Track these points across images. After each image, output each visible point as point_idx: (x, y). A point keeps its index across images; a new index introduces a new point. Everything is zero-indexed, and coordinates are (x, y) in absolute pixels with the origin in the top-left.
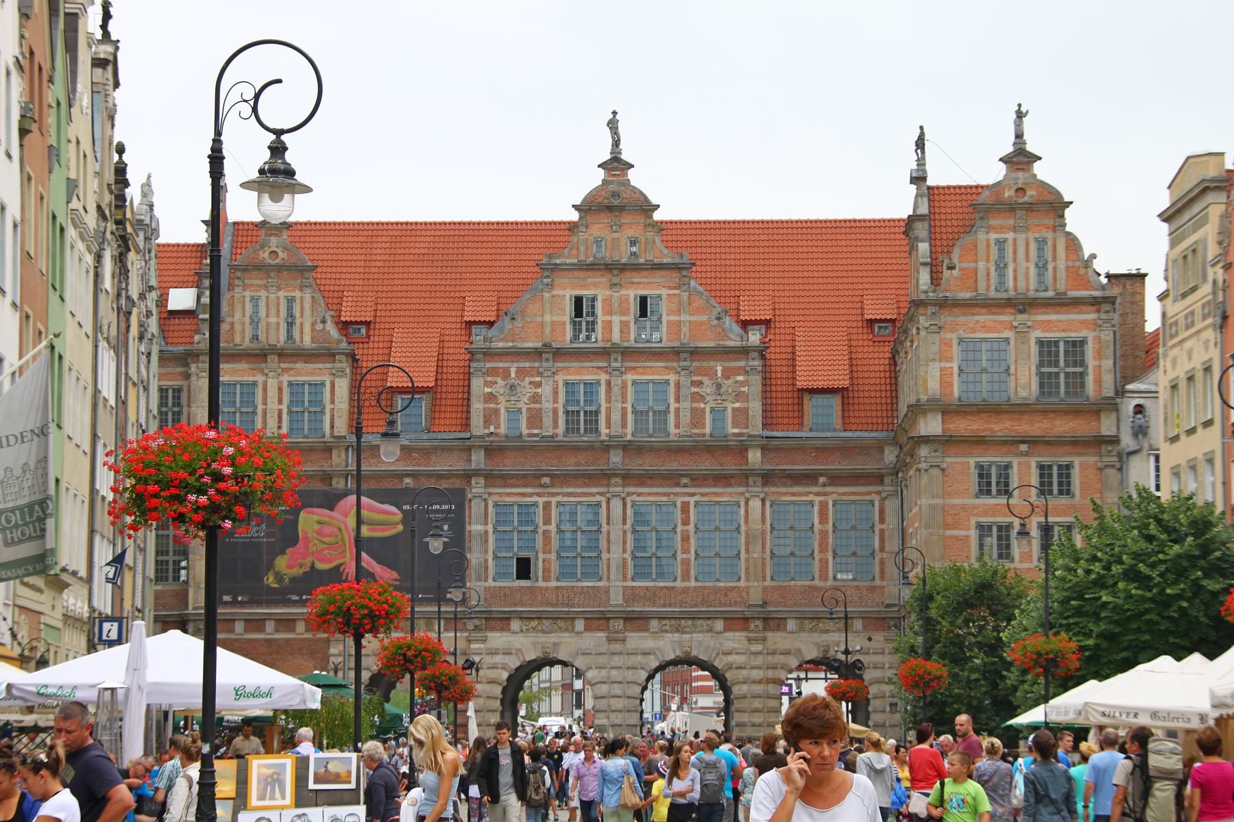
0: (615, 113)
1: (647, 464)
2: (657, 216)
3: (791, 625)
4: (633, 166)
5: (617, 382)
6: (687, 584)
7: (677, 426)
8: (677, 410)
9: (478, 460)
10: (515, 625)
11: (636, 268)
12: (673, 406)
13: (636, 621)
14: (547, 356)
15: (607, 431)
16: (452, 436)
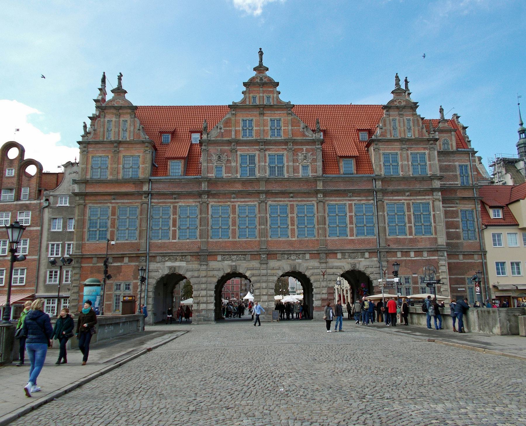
0: (261, 49)
1: (277, 188)
2: (278, 89)
3: (339, 256)
4: (267, 69)
5: (262, 154)
6: (294, 239)
7: (288, 172)
8: (288, 166)
9: (204, 187)
10: (219, 258)
11: (270, 107)
12: (286, 164)
13: (271, 255)
14: (233, 144)
15: (259, 175)
16: (193, 177)
